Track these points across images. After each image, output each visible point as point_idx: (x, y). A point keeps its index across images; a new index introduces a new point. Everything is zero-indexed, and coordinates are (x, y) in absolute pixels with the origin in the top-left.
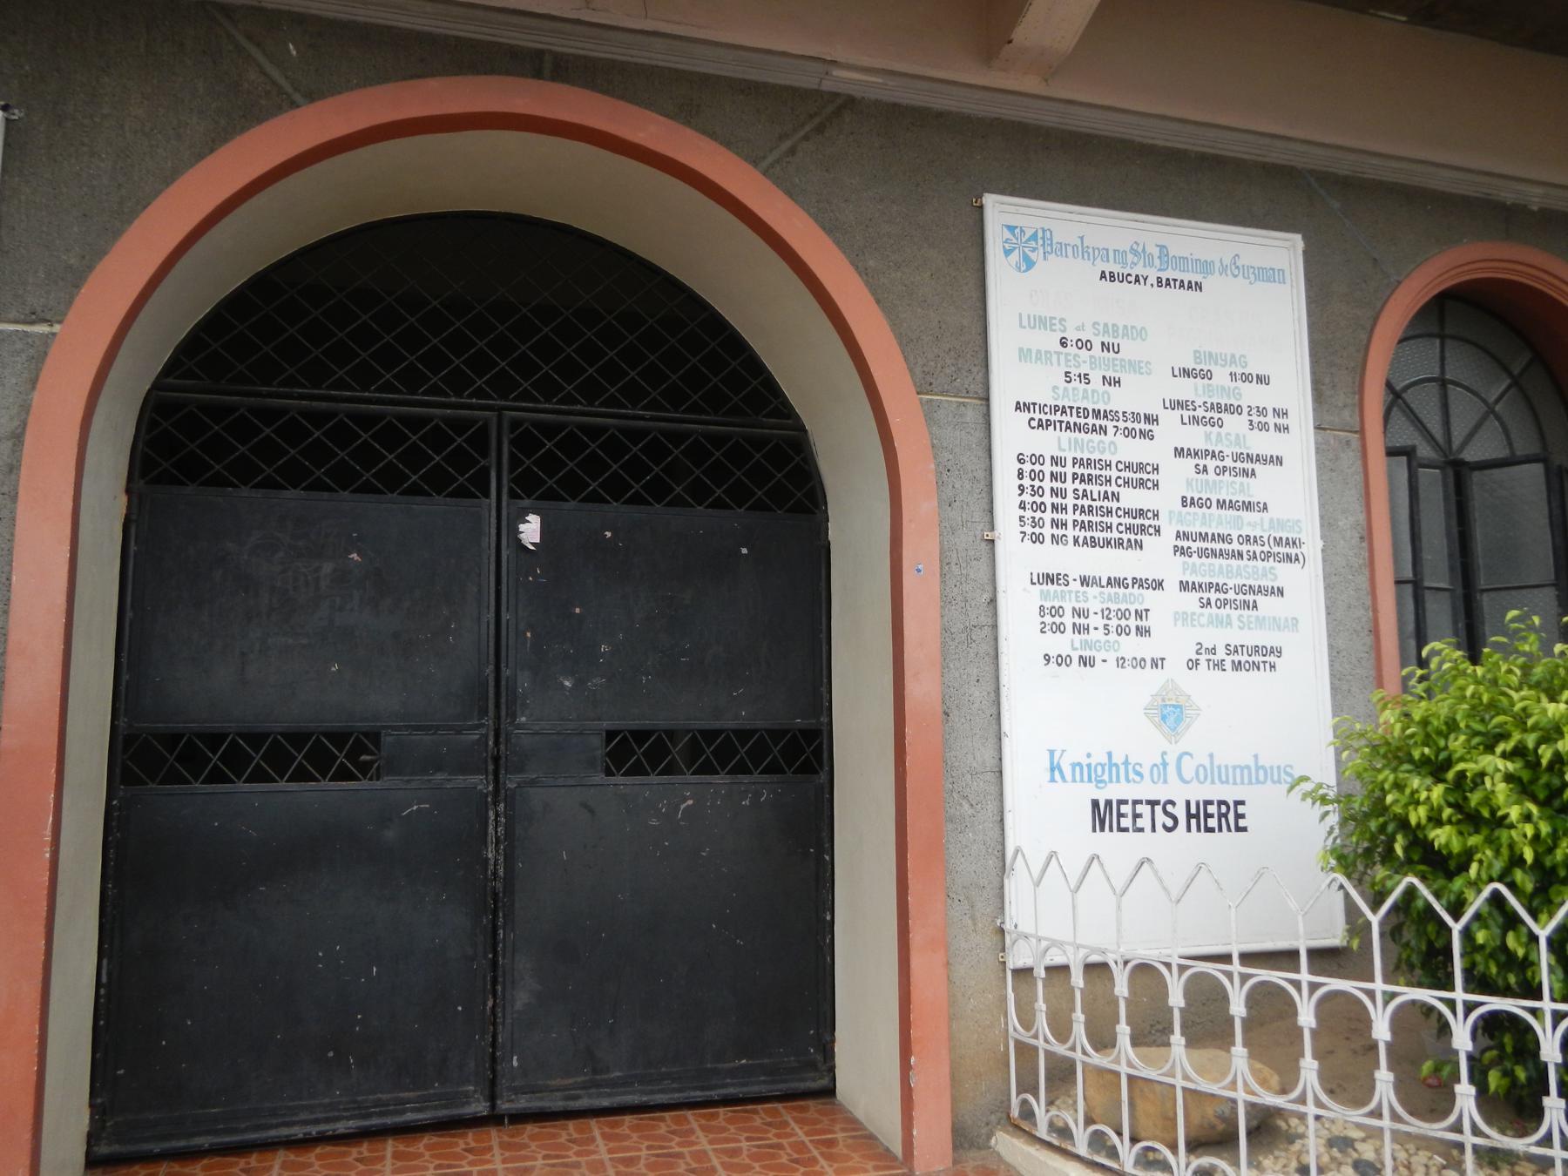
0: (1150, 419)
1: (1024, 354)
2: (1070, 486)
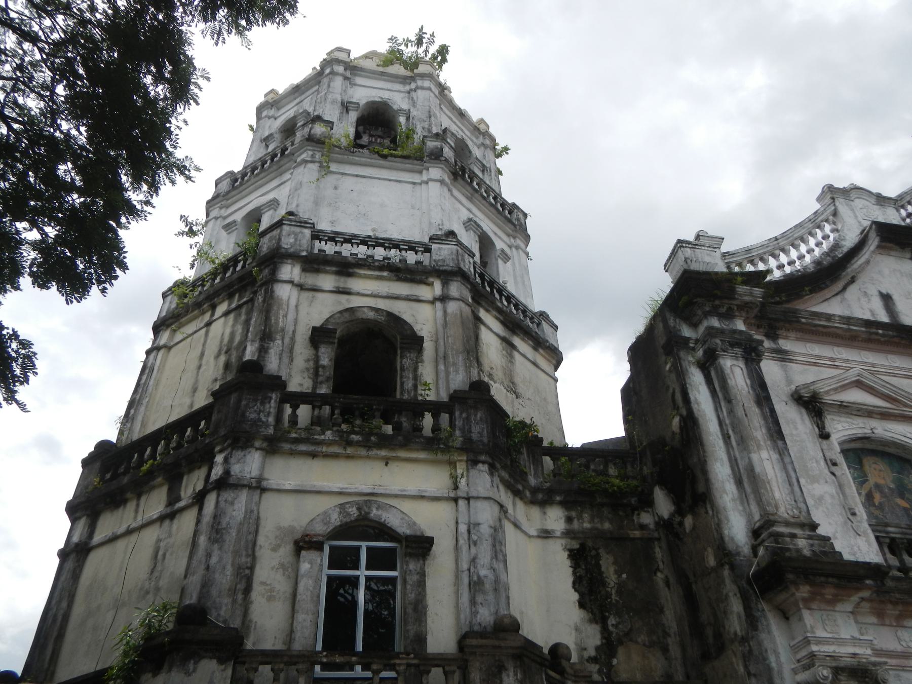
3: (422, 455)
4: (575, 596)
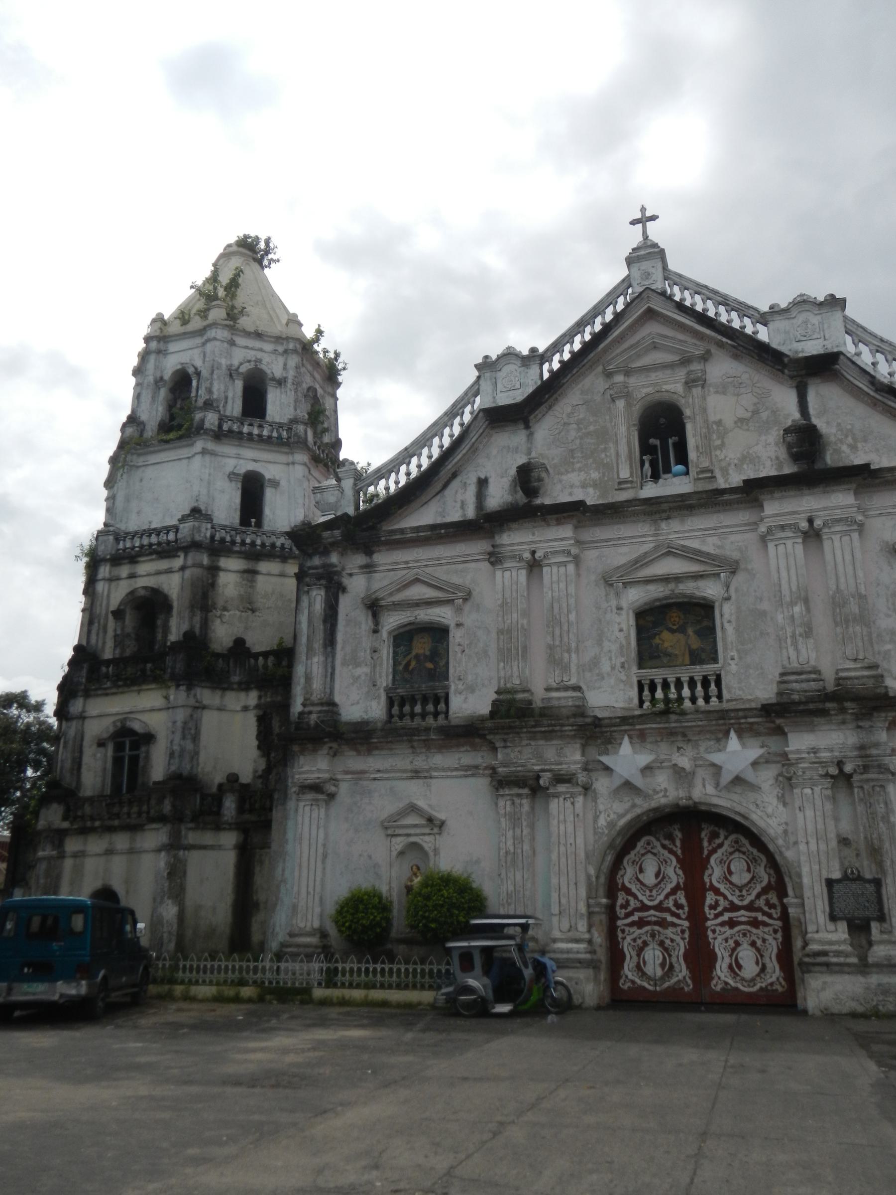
3: (153, 686)
4: (256, 743)
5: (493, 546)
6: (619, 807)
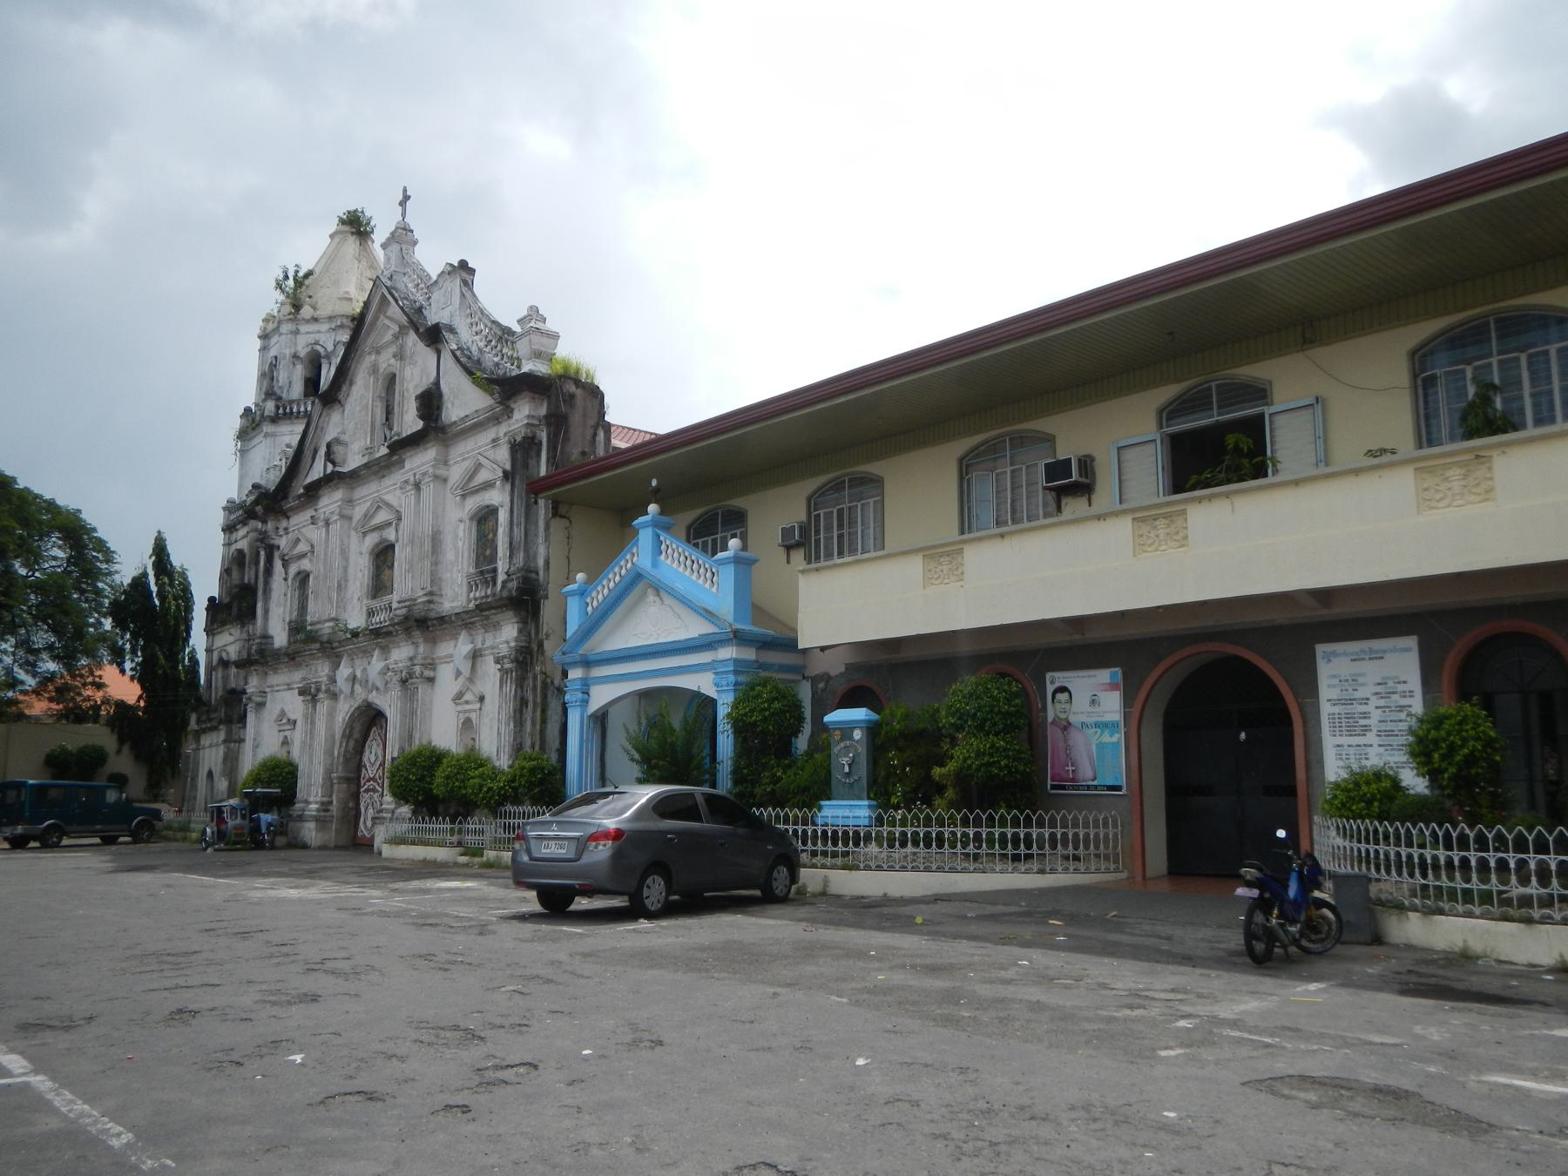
0: (1368, 699)
1: (1329, 686)
2: (1343, 720)
5: (316, 510)
6: (346, 707)
